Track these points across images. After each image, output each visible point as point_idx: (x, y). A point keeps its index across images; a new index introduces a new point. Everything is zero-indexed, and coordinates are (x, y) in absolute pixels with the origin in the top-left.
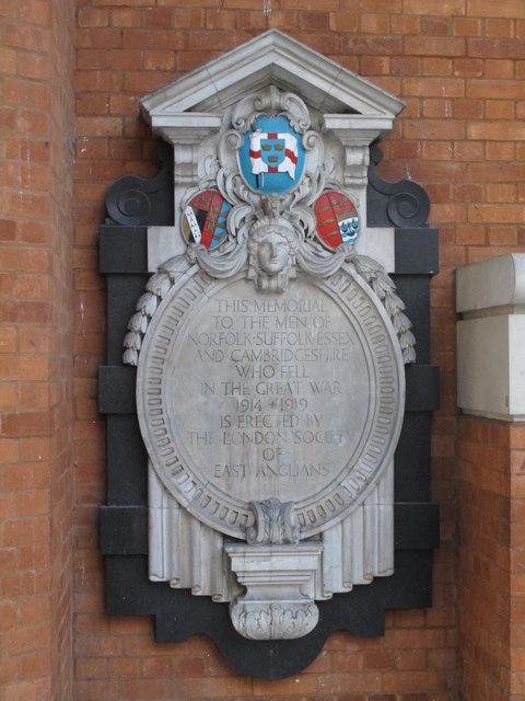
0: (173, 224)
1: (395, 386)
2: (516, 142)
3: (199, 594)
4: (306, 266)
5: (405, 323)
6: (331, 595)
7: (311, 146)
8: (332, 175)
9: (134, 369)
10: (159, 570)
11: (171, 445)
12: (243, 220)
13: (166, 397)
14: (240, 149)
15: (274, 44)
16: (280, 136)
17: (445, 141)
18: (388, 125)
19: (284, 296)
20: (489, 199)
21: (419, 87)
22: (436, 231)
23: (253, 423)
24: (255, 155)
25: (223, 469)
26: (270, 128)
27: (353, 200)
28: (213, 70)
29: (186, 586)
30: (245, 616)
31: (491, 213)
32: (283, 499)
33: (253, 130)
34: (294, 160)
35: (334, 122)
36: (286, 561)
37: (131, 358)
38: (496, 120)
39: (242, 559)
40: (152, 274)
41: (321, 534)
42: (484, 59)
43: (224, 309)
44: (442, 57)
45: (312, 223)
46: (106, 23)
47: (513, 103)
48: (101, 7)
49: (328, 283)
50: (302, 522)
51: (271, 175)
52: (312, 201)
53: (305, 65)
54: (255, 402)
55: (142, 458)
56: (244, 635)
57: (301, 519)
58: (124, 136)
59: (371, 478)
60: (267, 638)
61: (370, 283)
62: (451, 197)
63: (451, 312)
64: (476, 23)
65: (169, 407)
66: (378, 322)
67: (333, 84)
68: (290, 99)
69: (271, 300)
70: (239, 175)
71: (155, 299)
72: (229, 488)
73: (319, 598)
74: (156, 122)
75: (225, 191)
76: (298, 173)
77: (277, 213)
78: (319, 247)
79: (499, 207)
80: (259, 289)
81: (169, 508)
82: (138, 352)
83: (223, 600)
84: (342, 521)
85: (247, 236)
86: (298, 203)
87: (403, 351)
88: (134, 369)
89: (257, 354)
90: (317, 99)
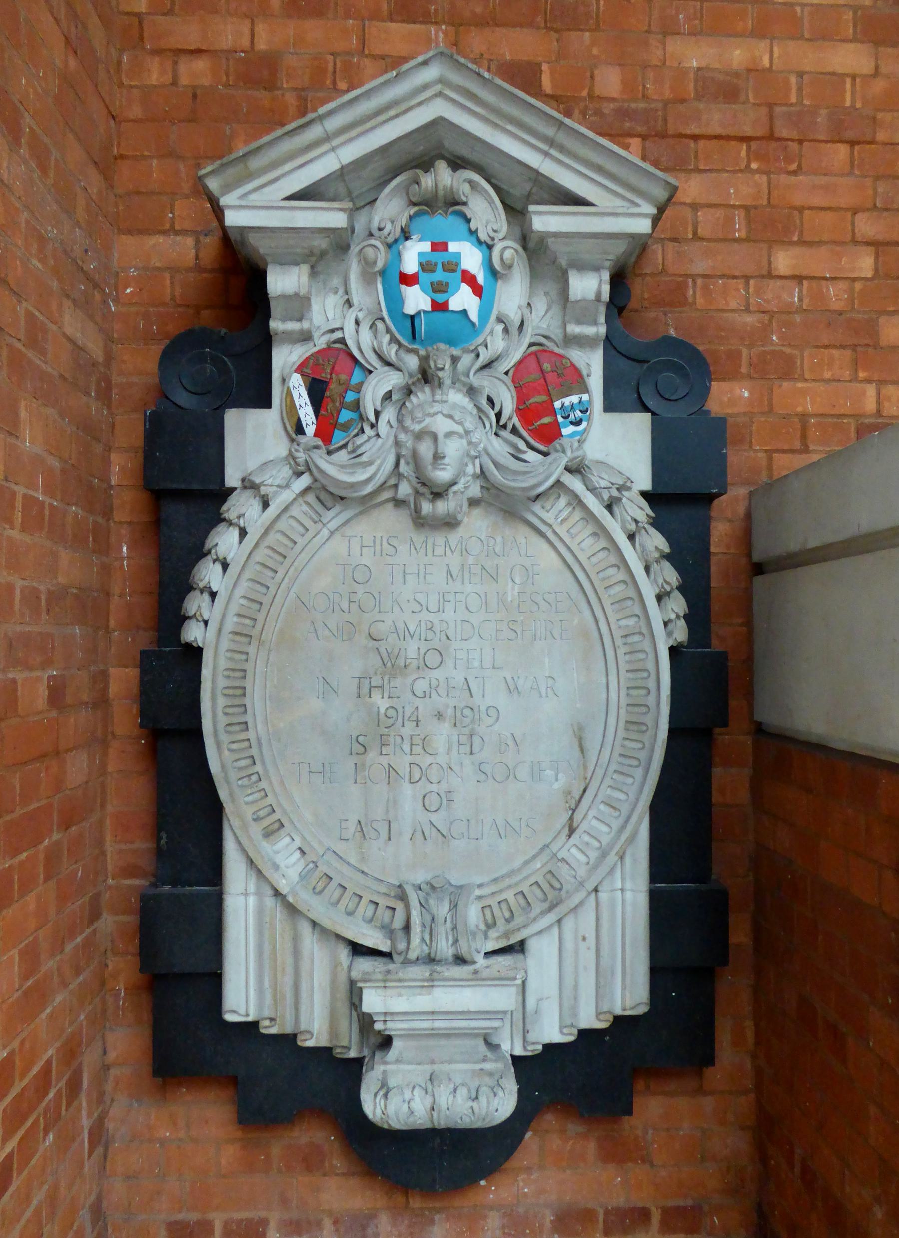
0: (267, 404)
1: (652, 684)
2: (854, 279)
3: (310, 1043)
4: (496, 475)
5: (670, 575)
6: (540, 1047)
7: (510, 267)
8: (543, 320)
9: (195, 654)
10: (241, 1000)
11: (263, 784)
12: (388, 396)
13: (256, 700)
14: (382, 272)
15: (440, 81)
16: (453, 247)
17: (734, 277)
18: (643, 226)
19: (461, 531)
20: (807, 376)
21: (692, 188)
22: (721, 422)
23: (406, 747)
24: (407, 280)
25: (352, 826)
26: (434, 247)
27: (581, 364)
28: (333, 124)
29: (288, 1030)
30: (386, 1096)
31: (806, 397)
32: (456, 878)
33: (406, 235)
34: (478, 290)
35: (546, 220)
36: (456, 997)
37: (193, 633)
38: (820, 243)
39: (380, 992)
40: (233, 490)
41: (522, 943)
42: (800, 142)
43: (356, 549)
44: (728, 138)
45: (508, 401)
46: (168, 78)
47: (849, 214)
48: (158, 52)
49: (537, 507)
50: (490, 920)
51: (438, 315)
52: (509, 363)
53: (496, 117)
54: (408, 711)
55: (211, 812)
56: (385, 1126)
57: (488, 912)
58: (198, 268)
59: (611, 846)
60: (428, 1125)
61: (609, 507)
62: (744, 370)
63: (743, 561)
64: (787, 82)
65: (259, 719)
66: (622, 575)
67: (546, 154)
68: (471, 182)
69: (439, 539)
70: (382, 319)
71: (235, 533)
72: (363, 859)
73: (519, 1051)
74: (233, 219)
75: (360, 350)
76: (484, 314)
77: (445, 376)
78: (522, 445)
79: (821, 389)
80: (420, 522)
81: (259, 893)
82: (206, 623)
83: (352, 1054)
84: (559, 921)
85: (394, 423)
86: (485, 367)
87: (666, 624)
88: (195, 654)
89: (412, 629)
90: (519, 188)
